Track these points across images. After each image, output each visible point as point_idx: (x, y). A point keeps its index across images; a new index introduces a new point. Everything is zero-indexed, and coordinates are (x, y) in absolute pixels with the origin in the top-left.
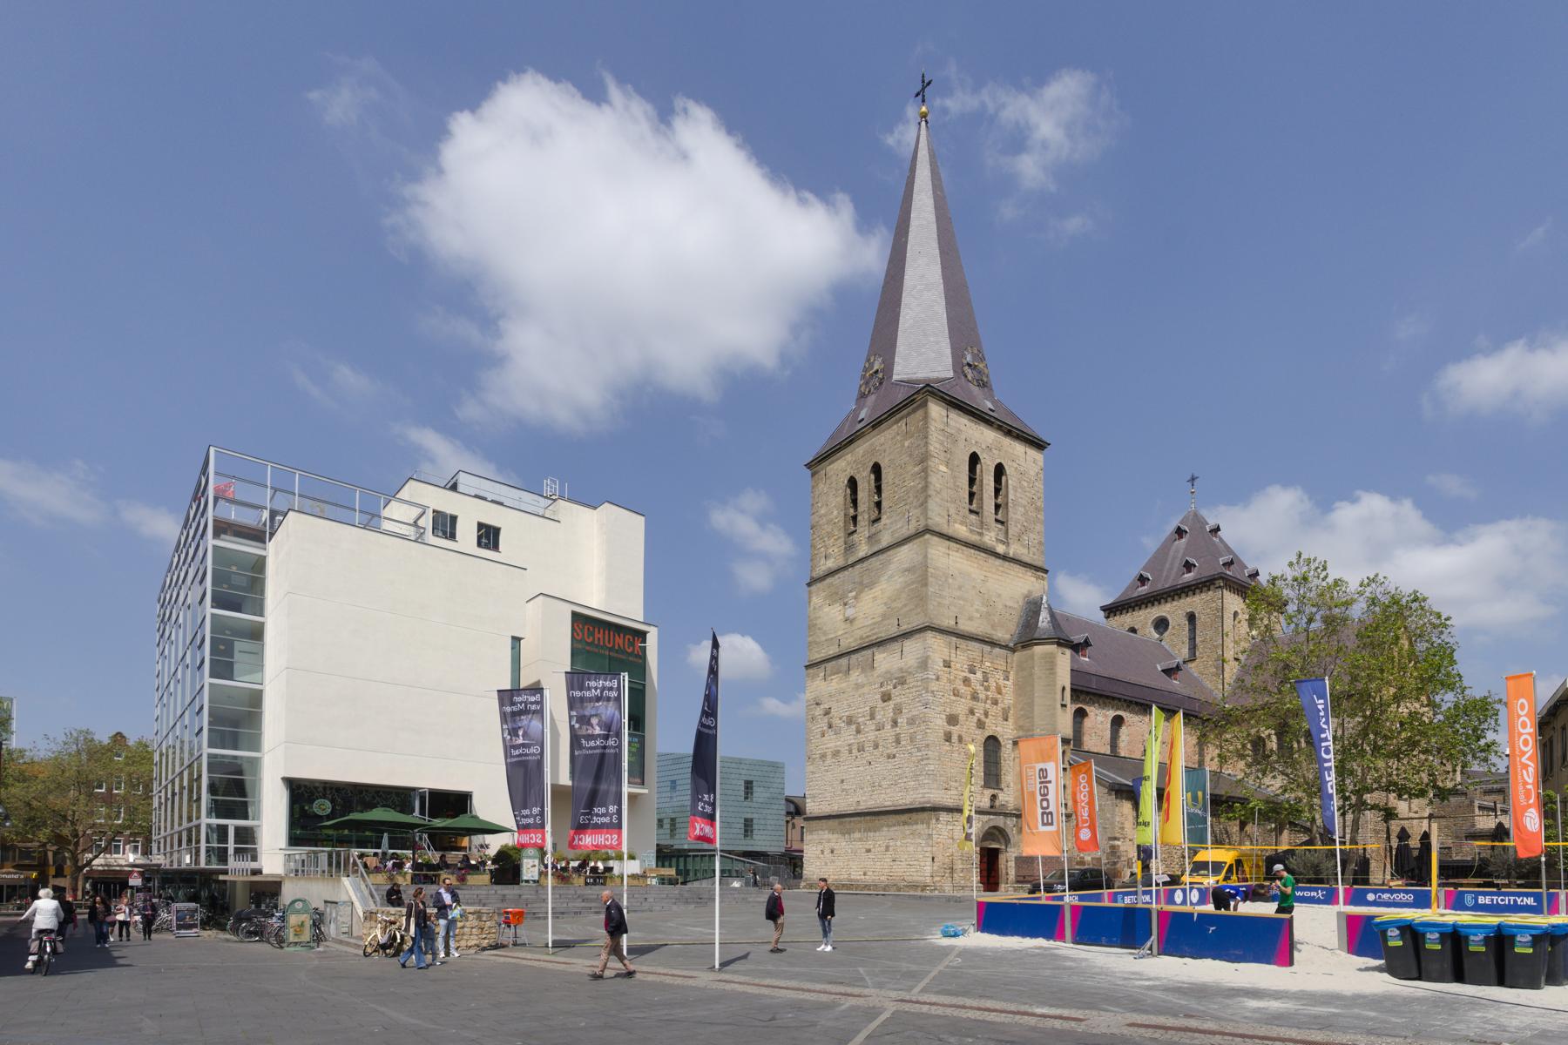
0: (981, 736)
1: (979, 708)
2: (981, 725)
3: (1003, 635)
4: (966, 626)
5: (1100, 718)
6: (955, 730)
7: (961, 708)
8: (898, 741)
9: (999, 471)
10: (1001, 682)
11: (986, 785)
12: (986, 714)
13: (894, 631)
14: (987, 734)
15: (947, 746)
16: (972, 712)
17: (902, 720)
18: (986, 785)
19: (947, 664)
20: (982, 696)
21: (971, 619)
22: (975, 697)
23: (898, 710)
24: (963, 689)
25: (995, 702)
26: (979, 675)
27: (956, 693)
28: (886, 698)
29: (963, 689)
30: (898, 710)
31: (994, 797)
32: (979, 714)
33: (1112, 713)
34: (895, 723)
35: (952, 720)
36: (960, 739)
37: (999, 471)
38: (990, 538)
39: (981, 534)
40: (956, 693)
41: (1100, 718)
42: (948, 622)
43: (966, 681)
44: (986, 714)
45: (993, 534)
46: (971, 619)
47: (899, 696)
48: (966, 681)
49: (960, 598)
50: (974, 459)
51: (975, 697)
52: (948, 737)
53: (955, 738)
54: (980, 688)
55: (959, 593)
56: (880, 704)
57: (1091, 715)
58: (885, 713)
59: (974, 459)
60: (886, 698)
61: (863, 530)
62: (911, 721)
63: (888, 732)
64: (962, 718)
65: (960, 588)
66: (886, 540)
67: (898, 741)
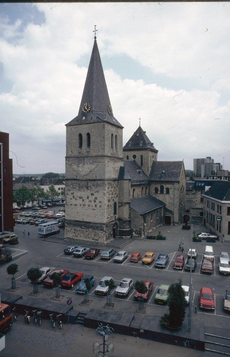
8: (96, 206)
23: (96, 198)
28: (92, 194)
30: (96, 198)
34: (95, 202)
56: (90, 196)
67: (96, 206)
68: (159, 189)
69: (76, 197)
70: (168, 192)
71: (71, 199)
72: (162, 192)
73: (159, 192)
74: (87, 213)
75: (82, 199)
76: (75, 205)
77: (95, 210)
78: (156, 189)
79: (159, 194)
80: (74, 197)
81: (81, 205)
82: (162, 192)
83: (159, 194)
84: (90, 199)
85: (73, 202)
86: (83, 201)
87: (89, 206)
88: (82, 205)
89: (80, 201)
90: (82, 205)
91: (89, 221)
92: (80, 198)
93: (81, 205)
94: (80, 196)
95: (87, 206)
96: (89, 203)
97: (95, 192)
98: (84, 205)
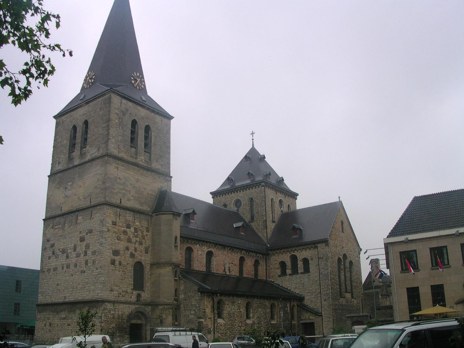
2: (132, 256)
3: (146, 208)
4: (126, 203)
5: (200, 252)
8: (86, 263)
11: (135, 288)
12: (136, 250)
13: (88, 204)
14: (136, 260)
16: (127, 249)
17: (89, 252)
18: (135, 288)
19: (114, 223)
20: (134, 240)
21: (129, 200)
22: (129, 240)
23: (88, 246)
26: (132, 229)
29: (122, 237)
30: (88, 246)
31: (139, 296)
32: (132, 250)
33: (206, 249)
34: (86, 254)
35: (116, 253)
36: (120, 263)
38: (141, 159)
39: (136, 158)
40: (119, 239)
41: (200, 252)
42: (115, 200)
43: (125, 232)
45: (142, 158)
47: (89, 239)
48: (125, 232)
49: (123, 189)
51: (129, 240)
52: (113, 262)
53: (117, 263)
55: (122, 187)
56: (79, 243)
57: (195, 251)
58: (81, 248)
60: (82, 239)
61: (77, 153)
62: (94, 253)
63: (82, 259)
64: (122, 252)
66: (88, 157)
67: (86, 263)
68: (289, 263)
69: (57, 251)
70: (307, 270)
71: (49, 258)
72: (295, 271)
73: (289, 271)
74: (71, 283)
75: (65, 255)
76: (55, 269)
77: (84, 272)
78: (283, 265)
79: (290, 275)
80: (54, 253)
81: (63, 268)
82: (295, 271)
83: (290, 275)
84: (78, 250)
85: (52, 264)
86: (67, 257)
87: (76, 266)
88: (65, 268)
89: (62, 259)
90: (65, 268)
91: (73, 299)
92: (64, 251)
93: (63, 268)
94: (62, 247)
95: (72, 267)
96: (77, 258)
97: (87, 234)
98: (68, 267)
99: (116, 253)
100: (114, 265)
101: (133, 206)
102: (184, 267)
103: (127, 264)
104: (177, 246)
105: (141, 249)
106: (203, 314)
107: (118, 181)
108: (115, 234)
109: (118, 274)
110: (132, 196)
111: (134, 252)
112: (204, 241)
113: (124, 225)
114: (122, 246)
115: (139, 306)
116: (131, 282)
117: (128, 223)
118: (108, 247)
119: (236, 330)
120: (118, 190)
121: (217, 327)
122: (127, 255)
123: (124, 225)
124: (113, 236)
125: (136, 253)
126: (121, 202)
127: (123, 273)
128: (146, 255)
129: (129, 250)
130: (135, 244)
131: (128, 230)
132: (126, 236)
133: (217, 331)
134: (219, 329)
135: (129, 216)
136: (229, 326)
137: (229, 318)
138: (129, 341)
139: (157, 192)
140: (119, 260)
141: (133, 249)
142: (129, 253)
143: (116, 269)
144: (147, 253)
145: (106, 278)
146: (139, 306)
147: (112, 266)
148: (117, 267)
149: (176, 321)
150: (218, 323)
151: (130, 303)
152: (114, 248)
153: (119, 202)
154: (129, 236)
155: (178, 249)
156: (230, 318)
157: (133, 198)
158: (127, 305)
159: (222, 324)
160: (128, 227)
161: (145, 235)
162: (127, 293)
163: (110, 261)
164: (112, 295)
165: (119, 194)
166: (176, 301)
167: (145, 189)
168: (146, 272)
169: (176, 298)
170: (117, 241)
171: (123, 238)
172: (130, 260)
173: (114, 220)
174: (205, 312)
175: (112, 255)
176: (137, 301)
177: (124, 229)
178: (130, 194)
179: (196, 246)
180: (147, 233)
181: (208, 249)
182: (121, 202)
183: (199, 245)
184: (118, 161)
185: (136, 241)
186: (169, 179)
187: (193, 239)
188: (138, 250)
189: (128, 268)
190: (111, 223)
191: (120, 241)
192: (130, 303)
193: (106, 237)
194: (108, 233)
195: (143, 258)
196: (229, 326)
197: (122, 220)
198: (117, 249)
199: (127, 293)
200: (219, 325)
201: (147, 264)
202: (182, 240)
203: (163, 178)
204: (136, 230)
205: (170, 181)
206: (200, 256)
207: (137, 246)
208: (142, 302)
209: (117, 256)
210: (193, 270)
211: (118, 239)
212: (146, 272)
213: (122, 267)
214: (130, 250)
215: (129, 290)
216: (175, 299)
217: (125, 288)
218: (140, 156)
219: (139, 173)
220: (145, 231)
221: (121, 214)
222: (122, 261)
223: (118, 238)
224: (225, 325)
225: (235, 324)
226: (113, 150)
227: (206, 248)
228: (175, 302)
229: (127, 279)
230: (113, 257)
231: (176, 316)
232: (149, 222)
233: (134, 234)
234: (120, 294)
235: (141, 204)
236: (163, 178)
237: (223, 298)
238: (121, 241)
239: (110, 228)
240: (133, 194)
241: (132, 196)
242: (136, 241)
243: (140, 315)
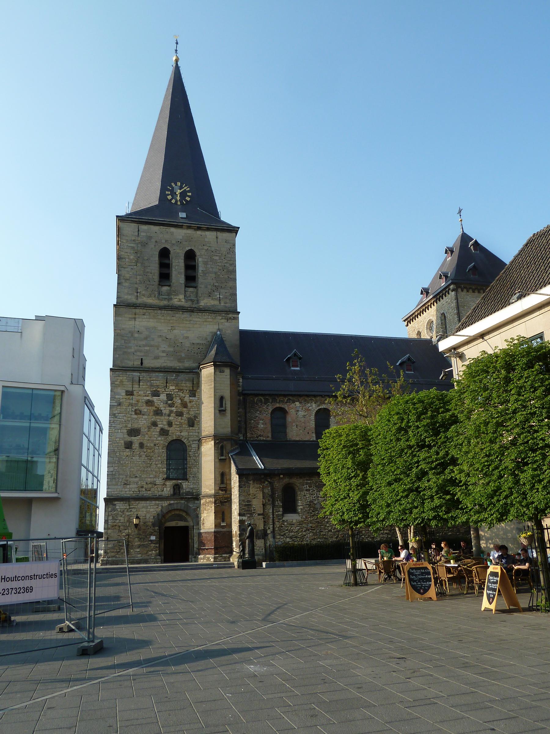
0: (162, 441)
1: (162, 423)
2: (164, 432)
4: (149, 363)
5: (301, 413)
6: (136, 440)
7: (142, 422)
9: (190, 256)
10: (187, 399)
12: (170, 424)
14: (170, 439)
15: (128, 452)
16: (155, 424)
20: (166, 411)
22: (158, 412)
24: (145, 409)
25: (180, 414)
26: (163, 397)
27: (138, 412)
29: (145, 409)
31: (177, 488)
33: (314, 407)
36: (141, 445)
37: (190, 256)
44: (170, 424)
46: (157, 358)
48: (149, 403)
50: (164, 254)
53: (136, 446)
54: (162, 406)
55: (144, 343)
59: (164, 254)
65: (146, 338)
99: (134, 432)
100: (131, 448)
101: (165, 365)
102: (269, 439)
103: (155, 445)
104: (225, 411)
105: (180, 422)
106: (244, 509)
107: (136, 335)
108: (130, 407)
109: (138, 460)
110: (163, 352)
111: (166, 427)
112: (308, 396)
113: (148, 392)
114: (145, 422)
115: (176, 502)
116: (161, 469)
117: (154, 389)
118: (119, 426)
119: (330, 531)
120: (136, 348)
121: (282, 527)
122: (153, 433)
123: (148, 392)
124: (128, 410)
125: (171, 429)
126: (142, 363)
127: (146, 458)
128: (191, 428)
129: (157, 426)
130: (169, 415)
131: (155, 399)
132: (150, 408)
133: (282, 534)
134: (287, 530)
135: (158, 380)
136: (310, 525)
137: (311, 511)
138: (158, 552)
139: (209, 339)
140: (139, 441)
141: (165, 423)
142: (158, 429)
143: (134, 454)
144: (193, 426)
145: (116, 468)
146: (176, 502)
147: (128, 450)
148: (136, 450)
149: (223, 521)
150: (283, 521)
151: (160, 498)
152: (130, 426)
153: (139, 363)
154: (158, 406)
155: (227, 414)
156: (313, 512)
157: (165, 354)
158: (153, 502)
159: (294, 521)
160: (156, 394)
161: (188, 401)
162: (155, 485)
163: (123, 444)
164: (127, 490)
165: (138, 354)
166: (222, 491)
167: (187, 338)
168: (190, 453)
169: (222, 486)
170: (136, 416)
171: (146, 410)
172: (160, 439)
173: (130, 389)
174: (250, 505)
175: (126, 436)
176: (174, 494)
177: (148, 398)
178: (158, 349)
179: (293, 405)
180: (191, 398)
181: (319, 406)
182: (142, 363)
183: (300, 403)
184: (134, 310)
185: (171, 412)
186: (235, 316)
187: (285, 396)
188: (173, 423)
189: (156, 451)
190: (124, 394)
191: (141, 416)
192: (160, 498)
193: (115, 414)
194: (119, 407)
195: (184, 434)
196: (310, 525)
197: (144, 387)
198: (136, 426)
199: (155, 485)
200: (286, 524)
201: (193, 441)
202: (263, 400)
203: (221, 318)
204: (170, 397)
205: (237, 319)
206: (303, 420)
207: (171, 418)
208: (193, 495)
209: (135, 436)
210: (290, 441)
211: (136, 414)
212: (190, 453)
213: (145, 450)
214: (159, 426)
215: (159, 481)
216: (220, 488)
217: (151, 478)
218: (177, 295)
219: (174, 318)
220: (188, 396)
221: (141, 379)
222: (145, 442)
223: (138, 412)
224: (300, 523)
225: (326, 520)
226: (126, 297)
227: (314, 405)
228: (220, 492)
229: (155, 466)
230: (129, 439)
231: (223, 513)
232: (195, 382)
233: (167, 403)
234: (142, 487)
235: (180, 360)
236: (221, 318)
237: (297, 482)
238: (143, 415)
239: (121, 400)
240: (164, 349)
241: (163, 352)
242: (171, 412)
243: (184, 514)
